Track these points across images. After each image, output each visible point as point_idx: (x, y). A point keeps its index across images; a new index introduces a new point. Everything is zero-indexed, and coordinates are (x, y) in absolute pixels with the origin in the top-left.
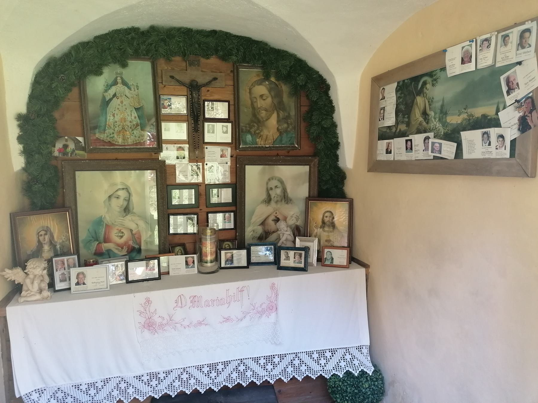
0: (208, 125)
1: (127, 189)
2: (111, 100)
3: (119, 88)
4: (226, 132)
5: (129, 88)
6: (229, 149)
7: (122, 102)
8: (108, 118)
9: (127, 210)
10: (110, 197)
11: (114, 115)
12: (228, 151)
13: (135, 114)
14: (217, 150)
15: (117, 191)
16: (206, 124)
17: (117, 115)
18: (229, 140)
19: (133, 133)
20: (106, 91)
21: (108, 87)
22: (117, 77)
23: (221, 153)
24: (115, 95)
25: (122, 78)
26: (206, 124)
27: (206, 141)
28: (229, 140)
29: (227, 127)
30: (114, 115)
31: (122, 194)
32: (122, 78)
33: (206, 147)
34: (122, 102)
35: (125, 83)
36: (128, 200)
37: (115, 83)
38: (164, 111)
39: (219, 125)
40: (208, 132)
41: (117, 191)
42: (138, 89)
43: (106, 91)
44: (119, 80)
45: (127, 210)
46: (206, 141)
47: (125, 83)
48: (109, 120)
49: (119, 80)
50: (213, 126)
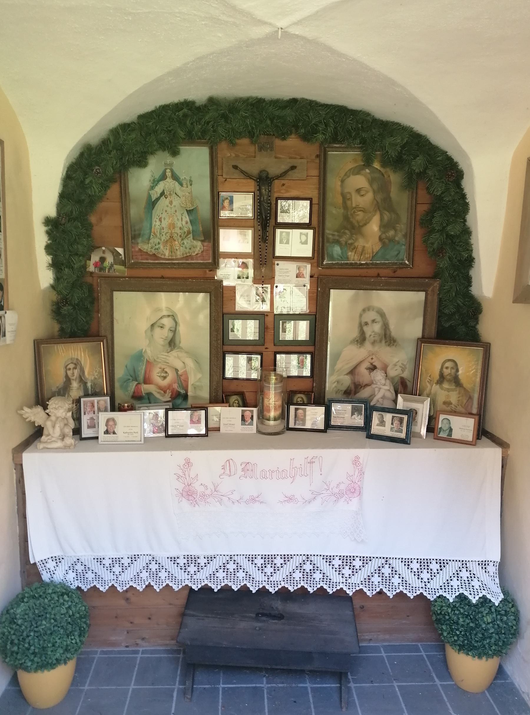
0: (281, 233)
1: (173, 316)
2: (158, 199)
3: (169, 184)
4: (306, 243)
5: (181, 185)
6: (309, 266)
7: (171, 203)
8: (154, 223)
9: (172, 343)
10: (153, 326)
11: (160, 220)
12: (307, 269)
13: (186, 218)
14: (292, 267)
15: (161, 318)
16: (278, 231)
17: (164, 219)
18: (309, 254)
19: (183, 244)
20: (152, 188)
21: (155, 183)
22: (166, 169)
23: (298, 272)
24: (162, 194)
25: (172, 171)
26: (278, 231)
27: (277, 254)
28: (309, 254)
29: (307, 235)
30: (160, 220)
31: (167, 322)
32: (172, 171)
33: (276, 262)
34: (171, 203)
35: (175, 177)
36: (174, 331)
37: (163, 177)
38: (224, 214)
39: (296, 232)
40: (281, 242)
41: (161, 318)
42: (191, 185)
43: (152, 188)
44: (169, 174)
45: (172, 343)
46: (277, 254)
47: (175, 177)
48: (155, 226)
49: (169, 174)
50: (288, 234)
